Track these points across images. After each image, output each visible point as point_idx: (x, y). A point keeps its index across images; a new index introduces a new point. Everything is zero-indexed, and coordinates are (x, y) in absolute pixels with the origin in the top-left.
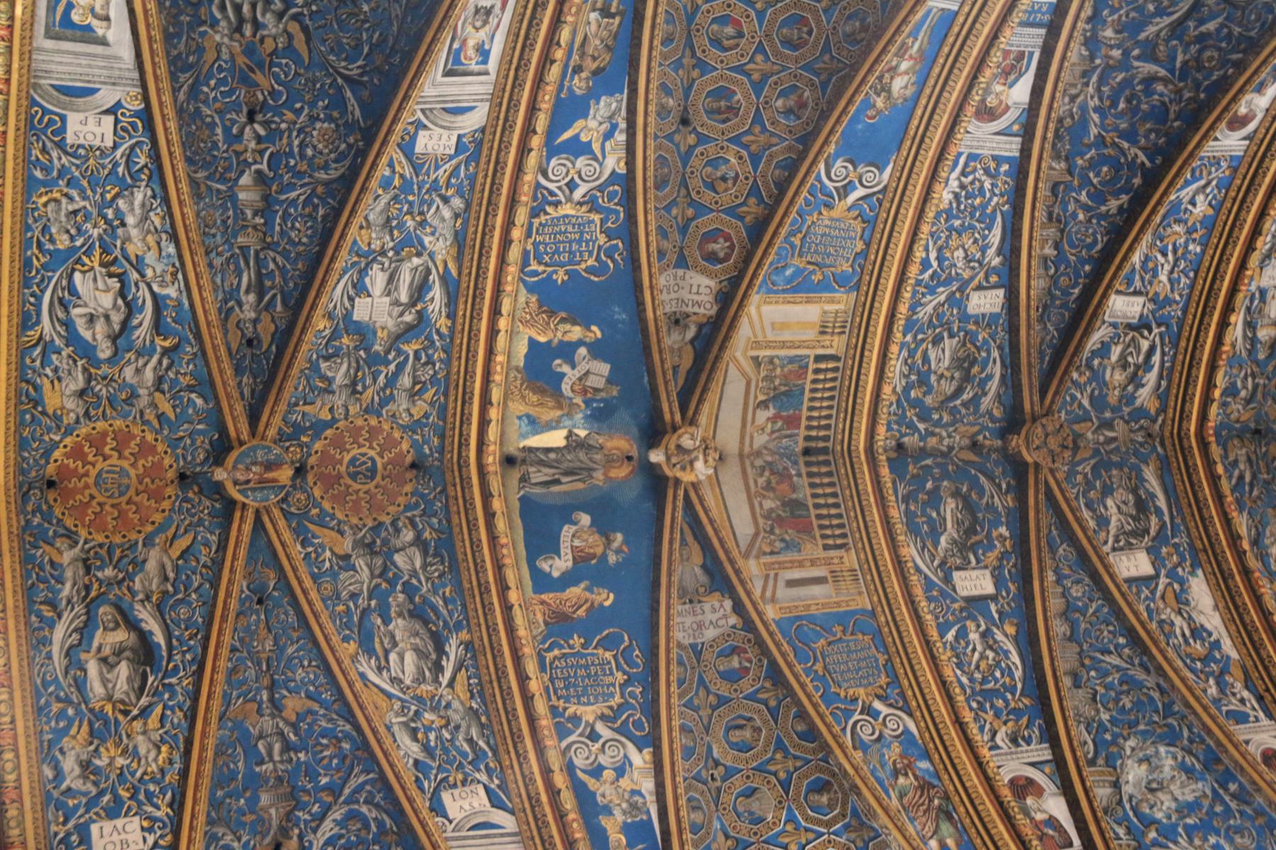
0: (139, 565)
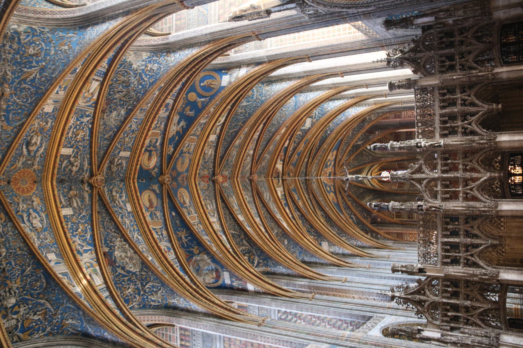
0: (23, 164)
